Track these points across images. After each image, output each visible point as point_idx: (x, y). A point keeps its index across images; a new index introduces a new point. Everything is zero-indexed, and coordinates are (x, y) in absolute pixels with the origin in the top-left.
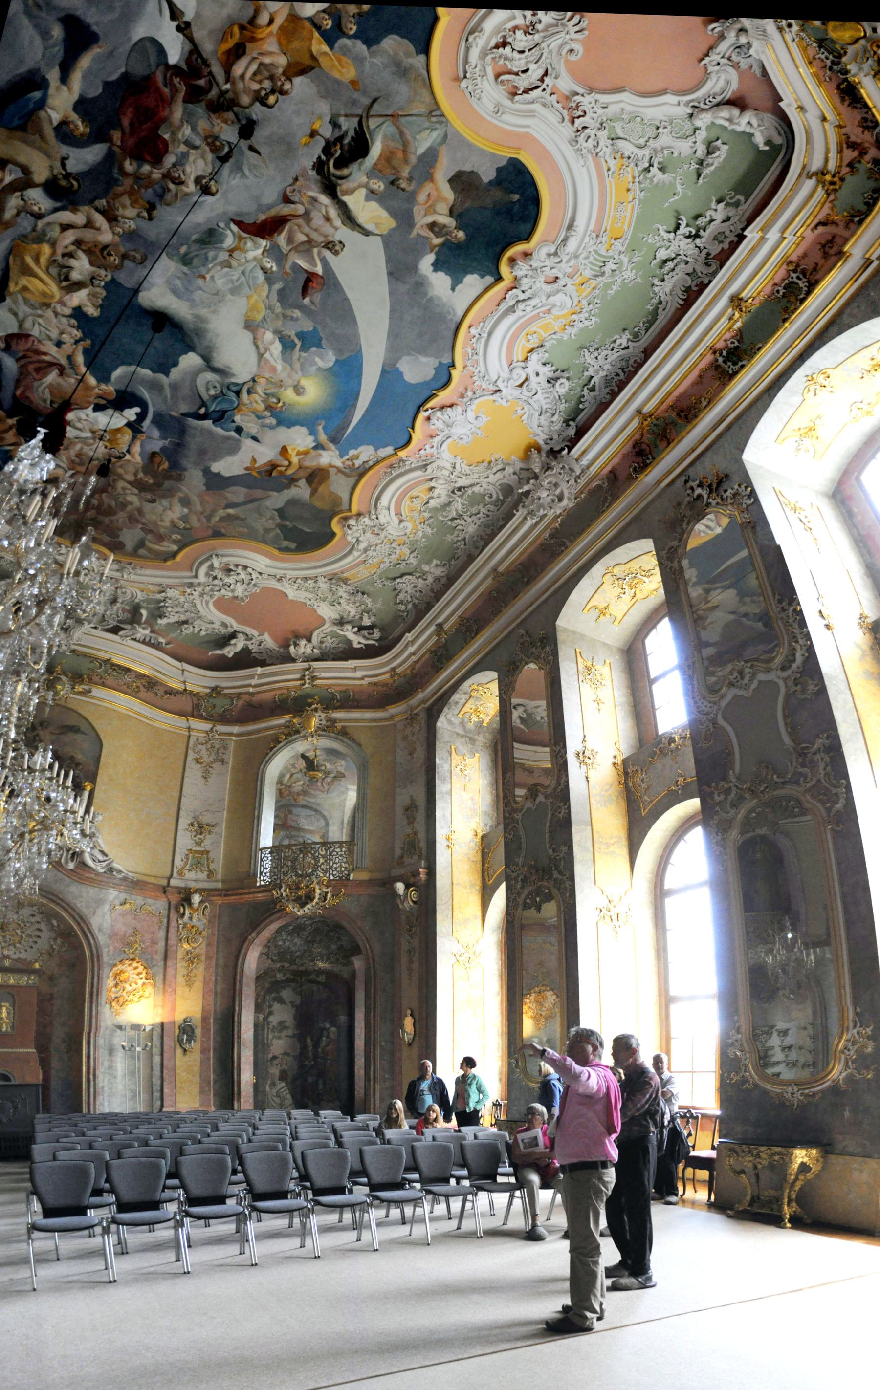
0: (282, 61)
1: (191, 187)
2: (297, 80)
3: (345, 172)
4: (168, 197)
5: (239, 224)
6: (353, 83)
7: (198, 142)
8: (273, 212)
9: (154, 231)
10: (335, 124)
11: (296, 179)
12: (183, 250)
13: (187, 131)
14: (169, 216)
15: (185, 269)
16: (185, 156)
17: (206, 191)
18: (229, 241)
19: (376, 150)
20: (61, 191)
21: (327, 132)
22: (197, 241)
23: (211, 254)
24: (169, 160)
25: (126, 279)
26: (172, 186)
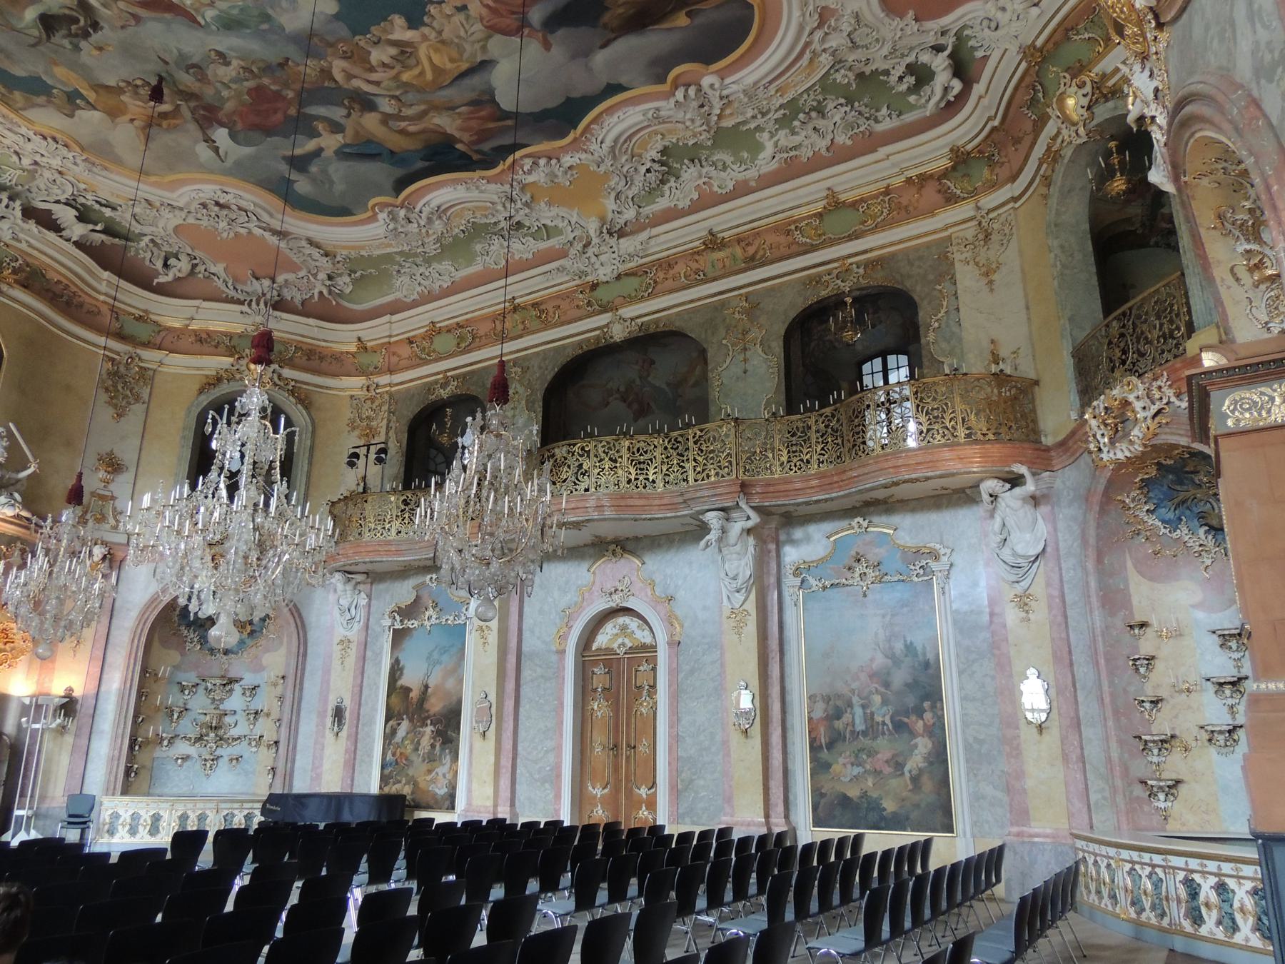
0: (124, 98)
1: (235, 63)
2: (112, 83)
3: (67, 12)
4: (262, 65)
5: (194, 20)
6: (56, 64)
7: (218, 85)
8: (153, 15)
9: (292, 51)
10: (77, 48)
11: (122, 27)
12: (265, 26)
13: (225, 93)
14: (271, 54)
15: (270, 12)
16: (234, 81)
17: (221, 55)
18: (210, 14)
19: (31, 14)
20: (366, 103)
21: (83, 44)
22: (248, 27)
23: (235, 12)
24: (251, 84)
25: (344, 31)
26: (255, 70)
